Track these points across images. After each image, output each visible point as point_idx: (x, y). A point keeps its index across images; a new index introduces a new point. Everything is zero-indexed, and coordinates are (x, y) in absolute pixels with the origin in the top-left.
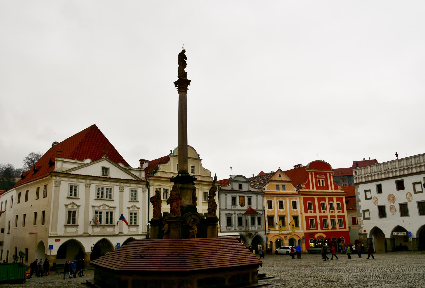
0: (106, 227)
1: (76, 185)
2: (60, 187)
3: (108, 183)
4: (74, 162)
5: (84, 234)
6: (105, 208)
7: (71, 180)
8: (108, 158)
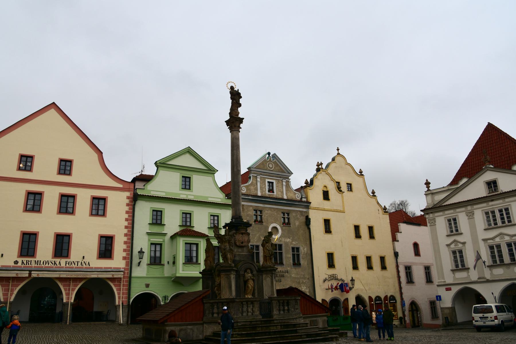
0: (512, 267)
1: (454, 217)
2: (436, 225)
3: (500, 201)
4: (445, 189)
5: (479, 279)
6: (503, 238)
7: (447, 212)
8: (491, 166)
